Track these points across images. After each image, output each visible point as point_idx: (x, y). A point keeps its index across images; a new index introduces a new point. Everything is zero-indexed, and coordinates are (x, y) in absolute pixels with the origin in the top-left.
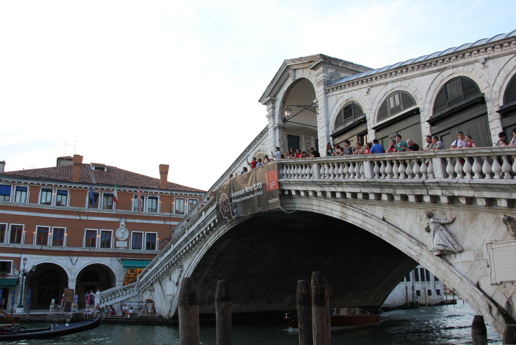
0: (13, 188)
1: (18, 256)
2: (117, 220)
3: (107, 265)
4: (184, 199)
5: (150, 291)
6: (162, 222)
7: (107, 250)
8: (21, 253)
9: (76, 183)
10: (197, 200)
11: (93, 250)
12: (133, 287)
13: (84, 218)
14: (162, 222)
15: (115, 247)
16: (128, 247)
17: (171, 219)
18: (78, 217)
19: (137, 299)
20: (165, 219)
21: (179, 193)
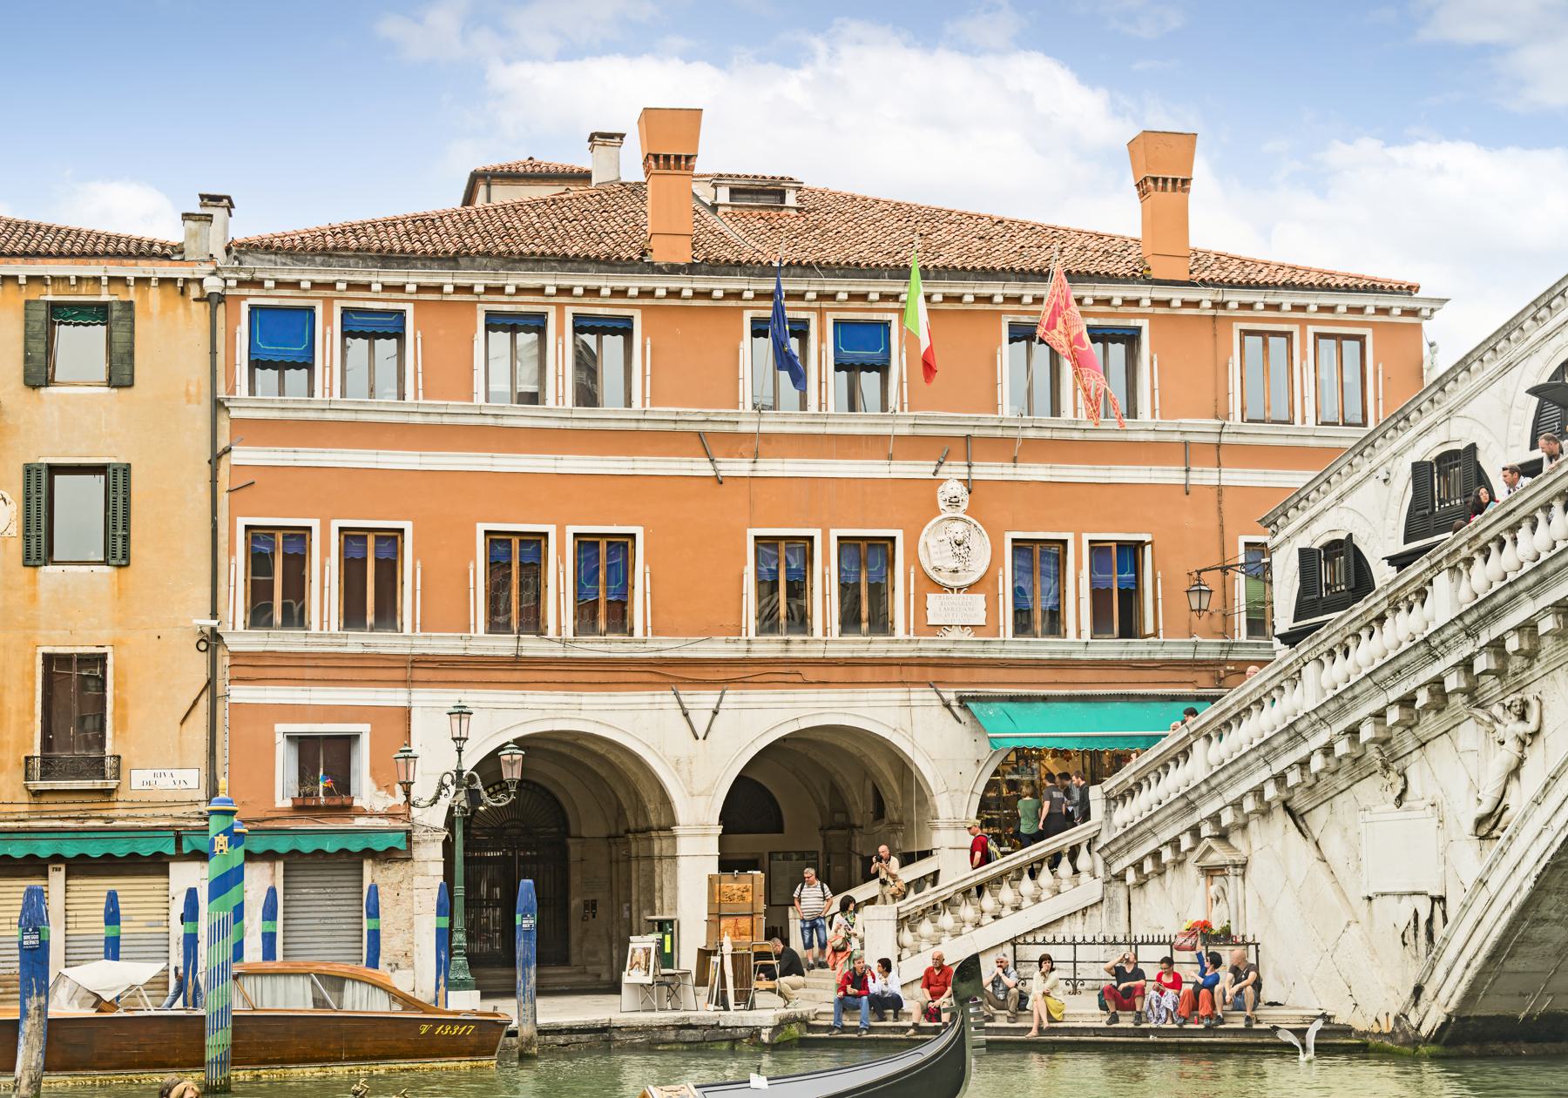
0: (328, 321)
1: (393, 697)
4: (1288, 335)
5: (1210, 872)
6: (1171, 475)
7: (877, 647)
8: (408, 683)
9: (674, 269)
10: (1361, 339)
11: (799, 647)
12: (1074, 853)
13: (736, 467)
14: (1171, 475)
16: (989, 628)
17: (1219, 453)
19: (1098, 925)
20: (1186, 453)
21: (1258, 298)
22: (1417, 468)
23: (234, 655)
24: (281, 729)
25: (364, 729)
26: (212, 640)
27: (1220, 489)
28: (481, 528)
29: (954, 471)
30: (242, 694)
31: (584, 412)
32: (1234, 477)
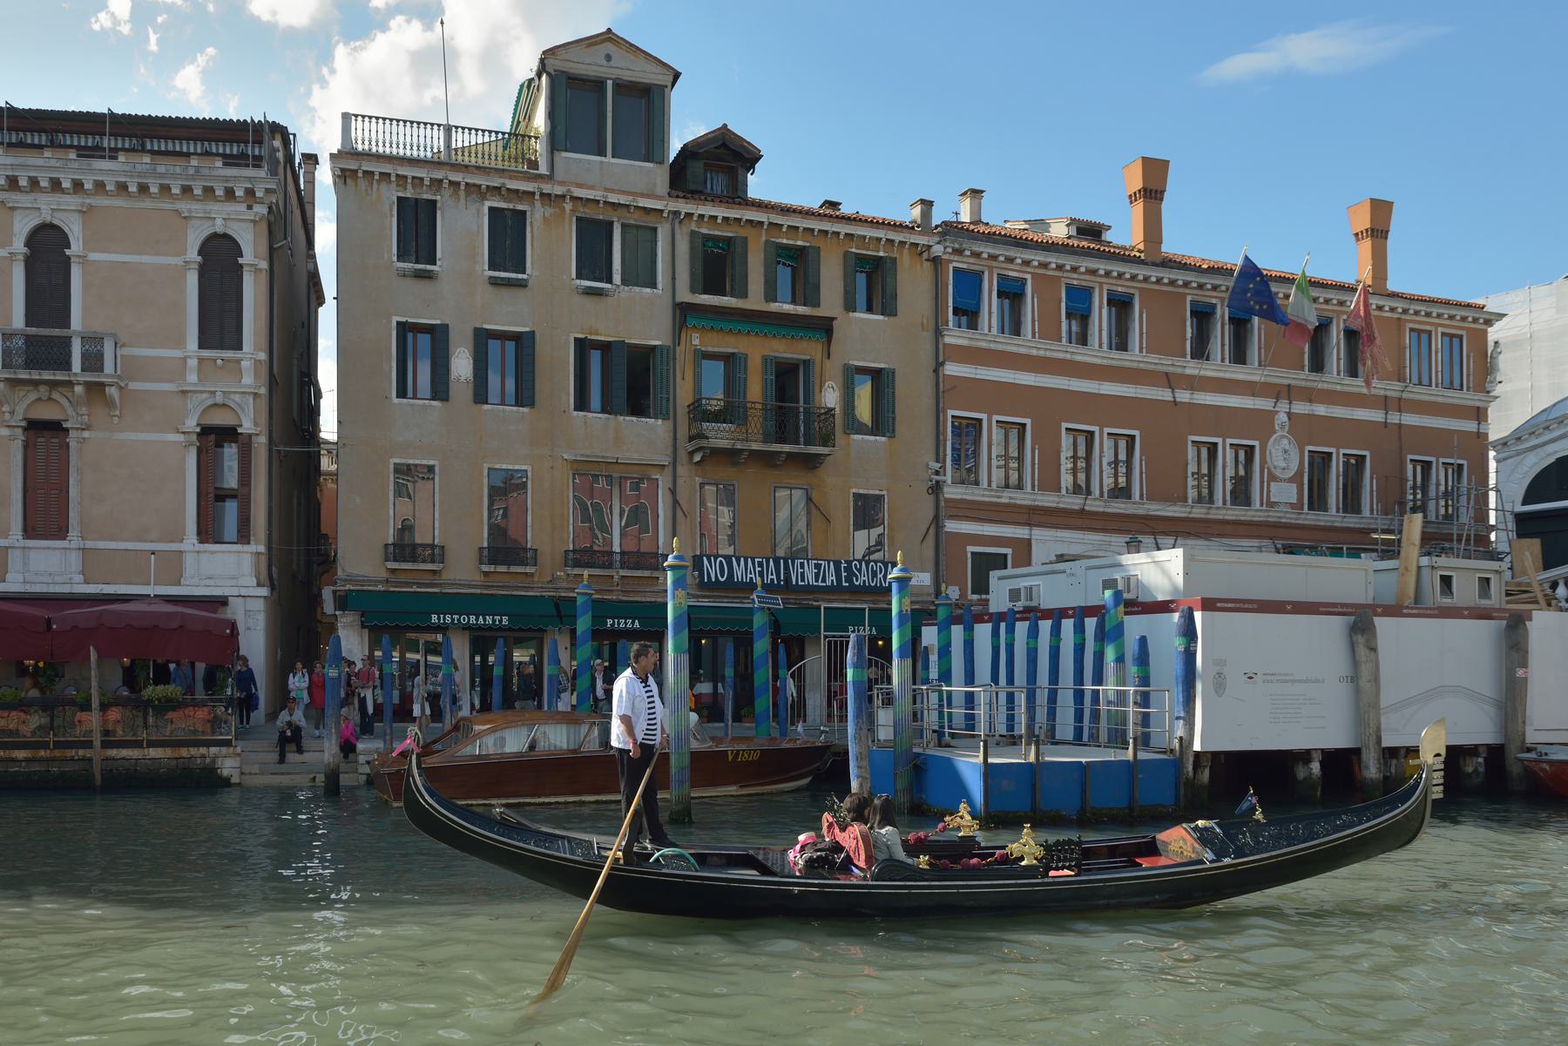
1: (1021, 532)
2: (1264, 404)
6: (1376, 416)
13: (1184, 396)
14: (1376, 416)
15: (1271, 504)
16: (1298, 506)
18: (1165, 395)
23: (947, 500)
24: (970, 549)
25: (1008, 551)
26: (936, 488)
27: (1400, 426)
28: (1028, 421)
29: (1283, 406)
30: (951, 526)
31: (1116, 354)
32: (1409, 419)
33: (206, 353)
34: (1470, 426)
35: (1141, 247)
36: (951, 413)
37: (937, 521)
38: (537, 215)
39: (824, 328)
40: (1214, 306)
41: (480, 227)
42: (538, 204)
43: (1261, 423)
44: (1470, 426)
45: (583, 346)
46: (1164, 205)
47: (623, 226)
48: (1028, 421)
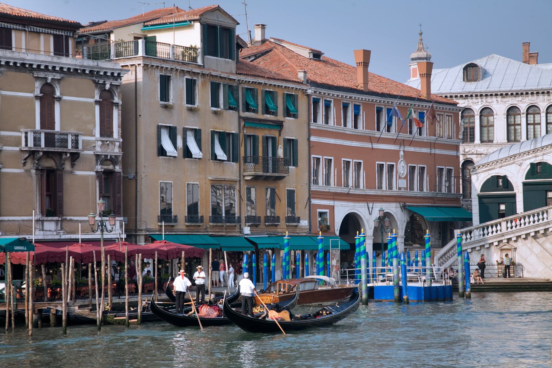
3: (393, 214)
8: (334, 199)
18: (369, 145)
22: (532, 164)
24: (319, 210)
25: (327, 211)
32: (438, 151)
33: (104, 139)
34: (453, 153)
35: (362, 85)
36: (312, 156)
37: (309, 199)
38: (199, 81)
39: (280, 125)
40: (382, 108)
41: (183, 86)
42: (200, 77)
43: (394, 155)
44: (453, 153)
45: (213, 133)
46: (369, 68)
47: (224, 85)
48: (332, 158)
